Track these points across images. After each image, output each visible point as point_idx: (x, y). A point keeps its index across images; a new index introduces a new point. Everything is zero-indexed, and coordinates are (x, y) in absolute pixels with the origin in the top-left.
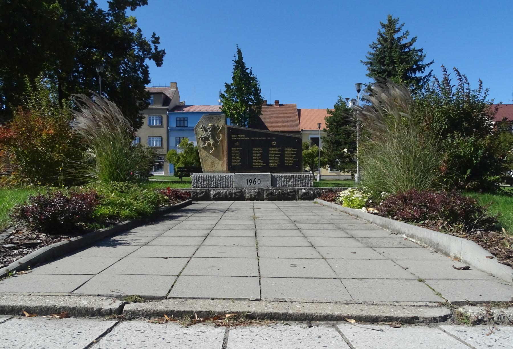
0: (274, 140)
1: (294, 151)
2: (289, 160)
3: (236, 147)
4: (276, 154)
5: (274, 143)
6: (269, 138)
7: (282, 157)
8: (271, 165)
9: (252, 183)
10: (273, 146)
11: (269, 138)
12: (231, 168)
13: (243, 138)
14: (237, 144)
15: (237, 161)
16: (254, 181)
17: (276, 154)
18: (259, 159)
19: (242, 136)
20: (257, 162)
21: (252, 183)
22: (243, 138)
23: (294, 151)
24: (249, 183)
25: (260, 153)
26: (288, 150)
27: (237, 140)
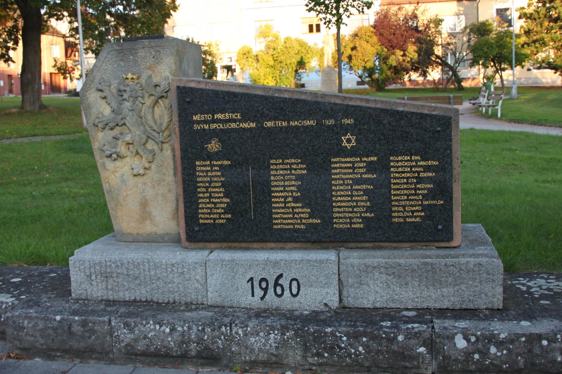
0: (346, 129)
1: (427, 169)
2: (407, 207)
3: (210, 157)
4: (357, 182)
5: (348, 141)
6: (331, 122)
7: (380, 197)
8: (340, 224)
9: (271, 290)
10: (343, 152)
11: (331, 122)
12: (197, 233)
13: (233, 125)
14: (214, 146)
15: (215, 206)
16: (276, 284)
17: (357, 182)
18: (296, 200)
19: (227, 116)
20: (286, 212)
21: (271, 290)
22: (233, 125)
23: (427, 169)
24: (259, 292)
25: (299, 178)
26: (402, 165)
27: (215, 133)
